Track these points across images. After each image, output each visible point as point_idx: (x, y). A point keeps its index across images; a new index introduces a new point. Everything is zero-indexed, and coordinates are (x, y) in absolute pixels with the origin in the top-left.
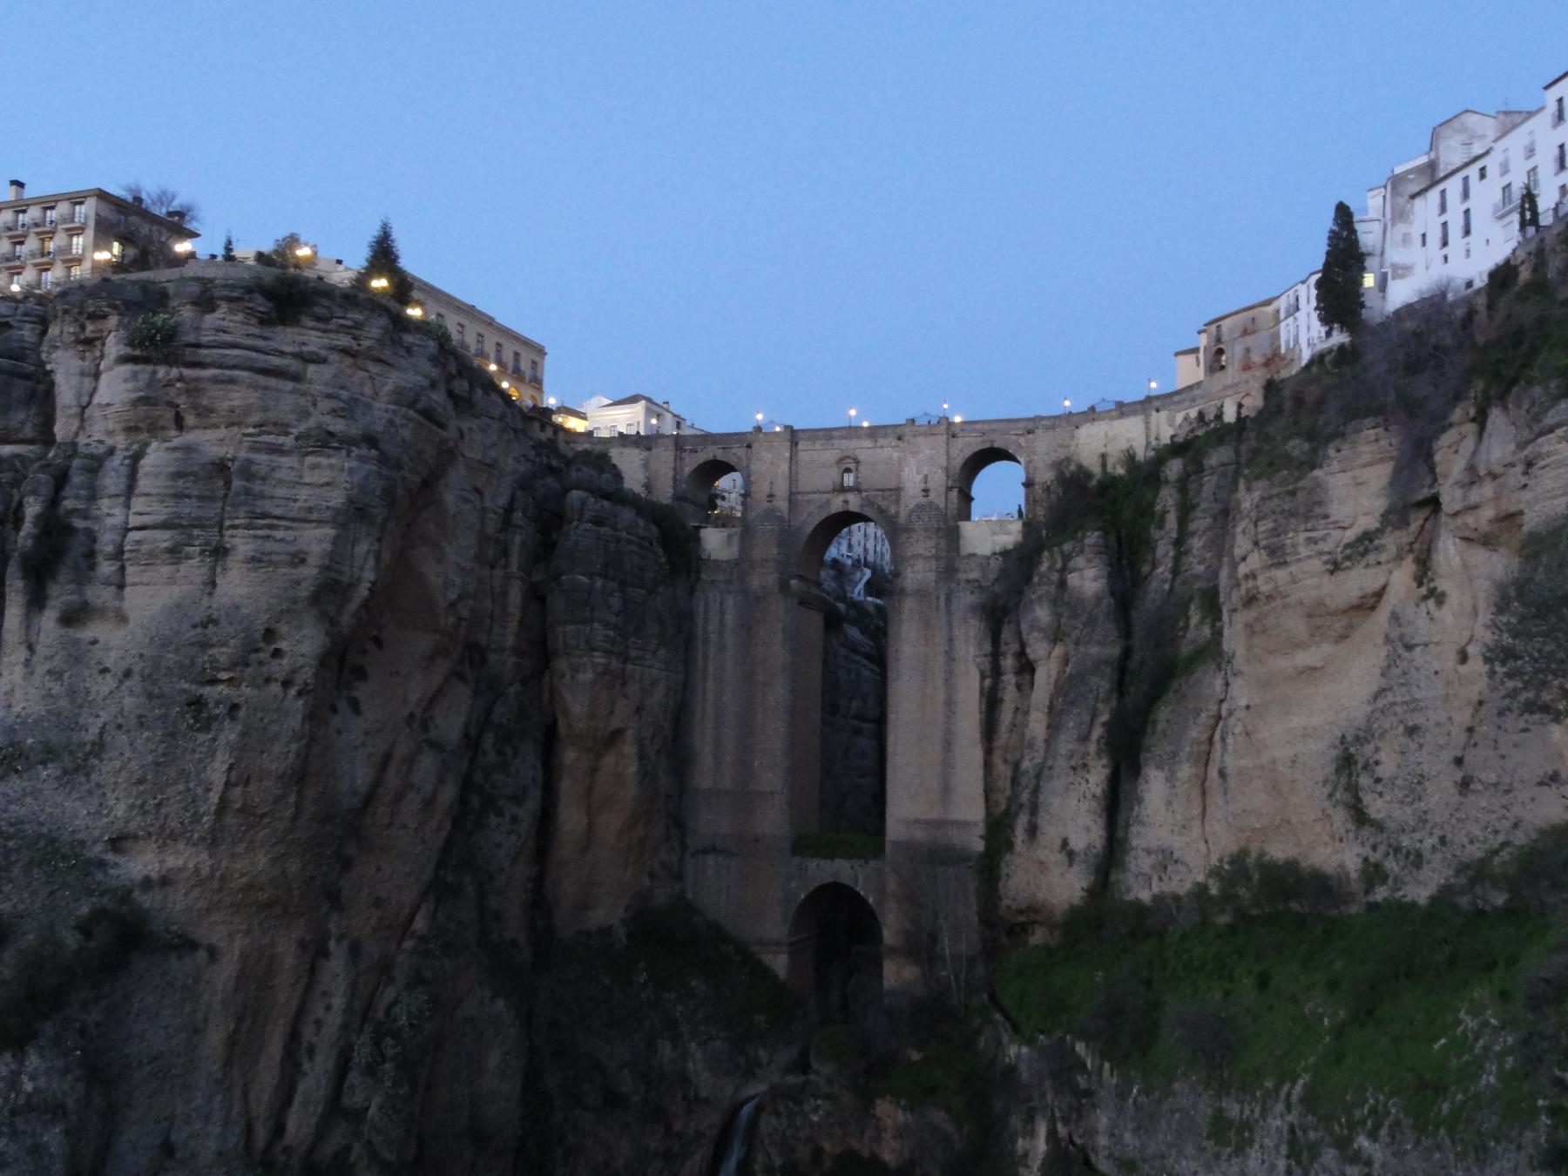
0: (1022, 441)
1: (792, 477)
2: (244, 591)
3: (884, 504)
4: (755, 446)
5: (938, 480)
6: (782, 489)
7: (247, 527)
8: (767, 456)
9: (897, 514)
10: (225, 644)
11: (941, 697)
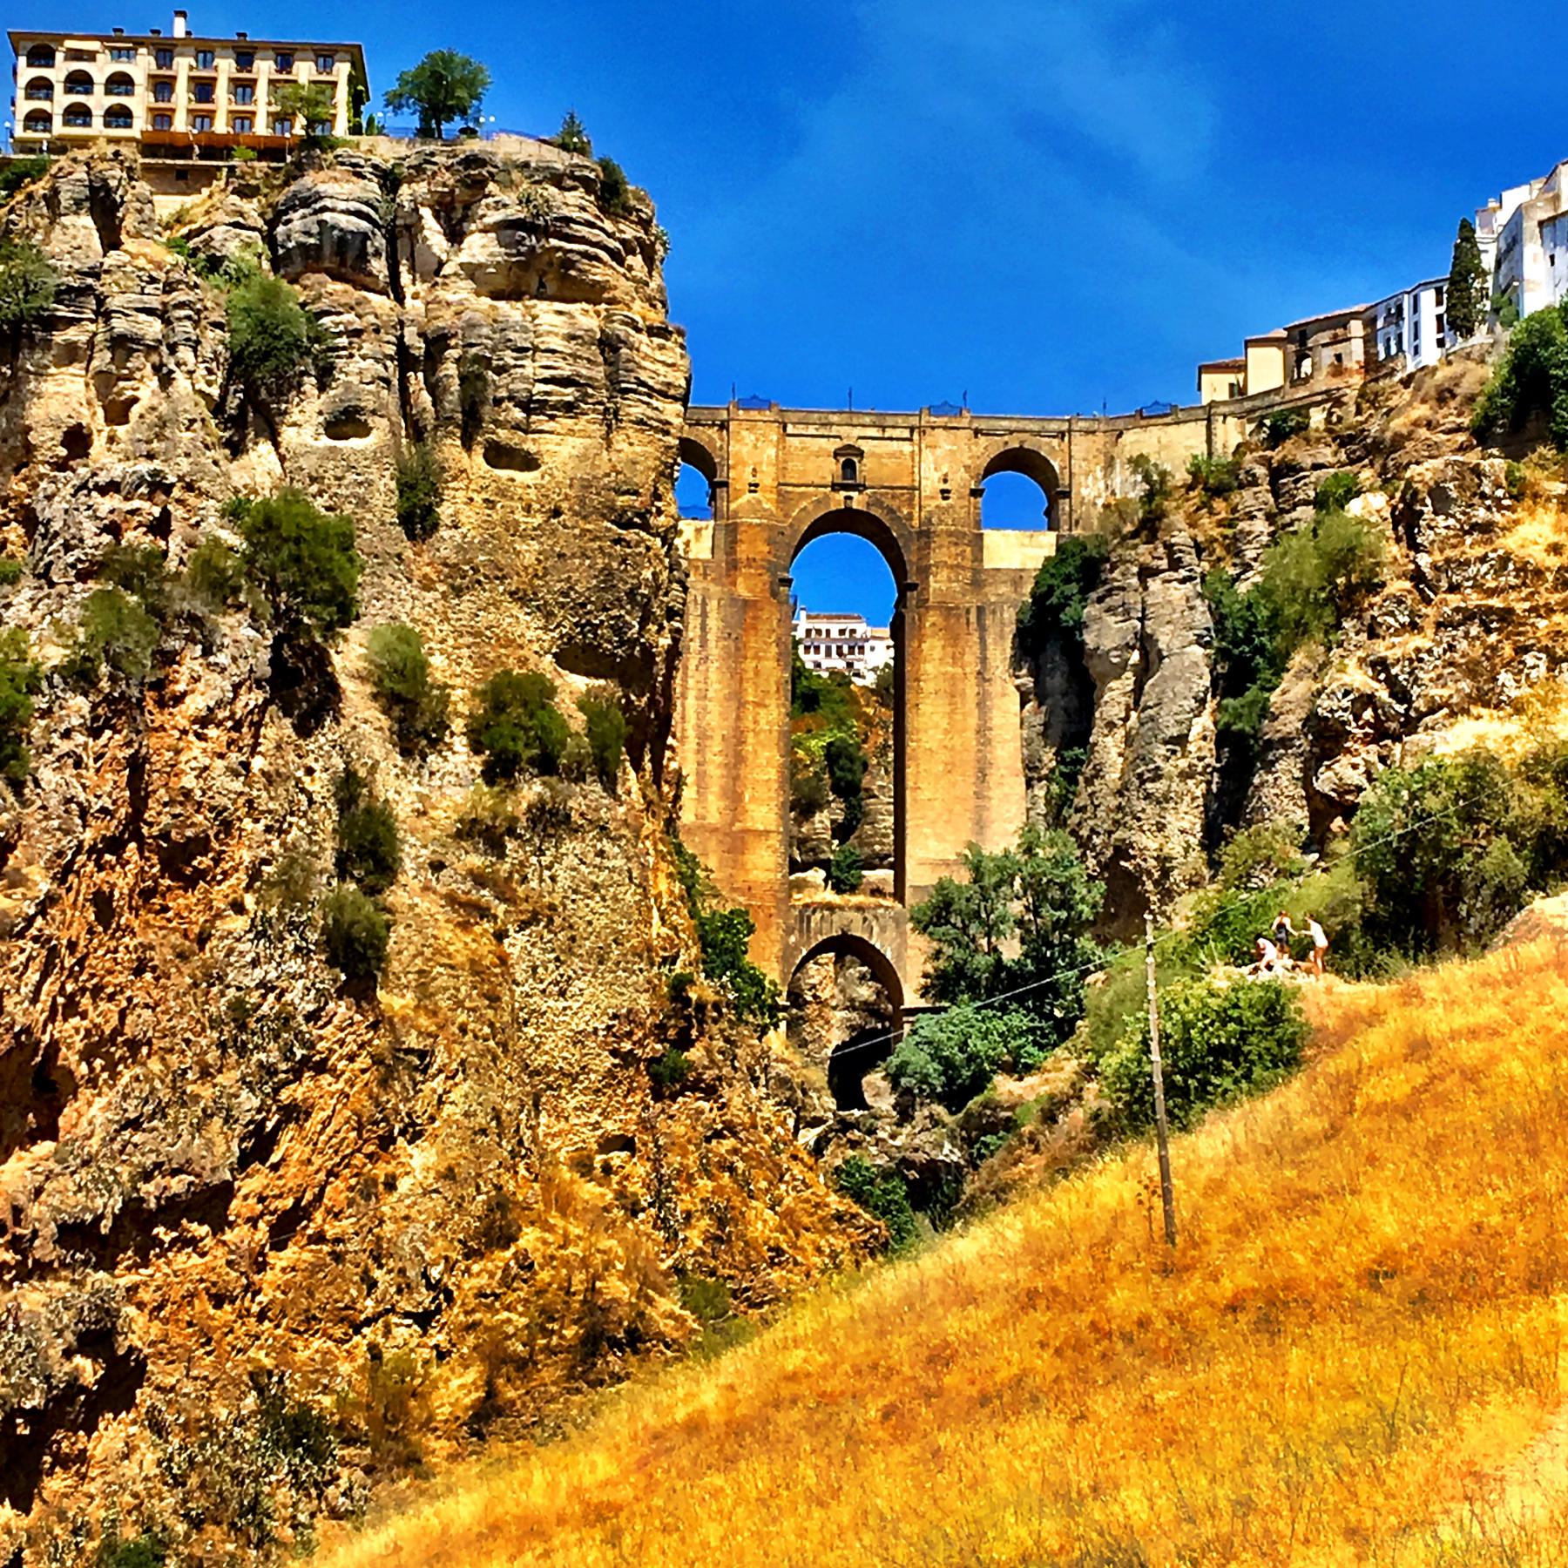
0: (1055, 442)
1: (781, 466)
2: (638, 449)
3: (895, 504)
4: (733, 425)
5: (961, 480)
6: (767, 479)
7: (635, 391)
8: (749, 438)
9: (910, 517)
10: (636, 493)
11: (973, 722)
